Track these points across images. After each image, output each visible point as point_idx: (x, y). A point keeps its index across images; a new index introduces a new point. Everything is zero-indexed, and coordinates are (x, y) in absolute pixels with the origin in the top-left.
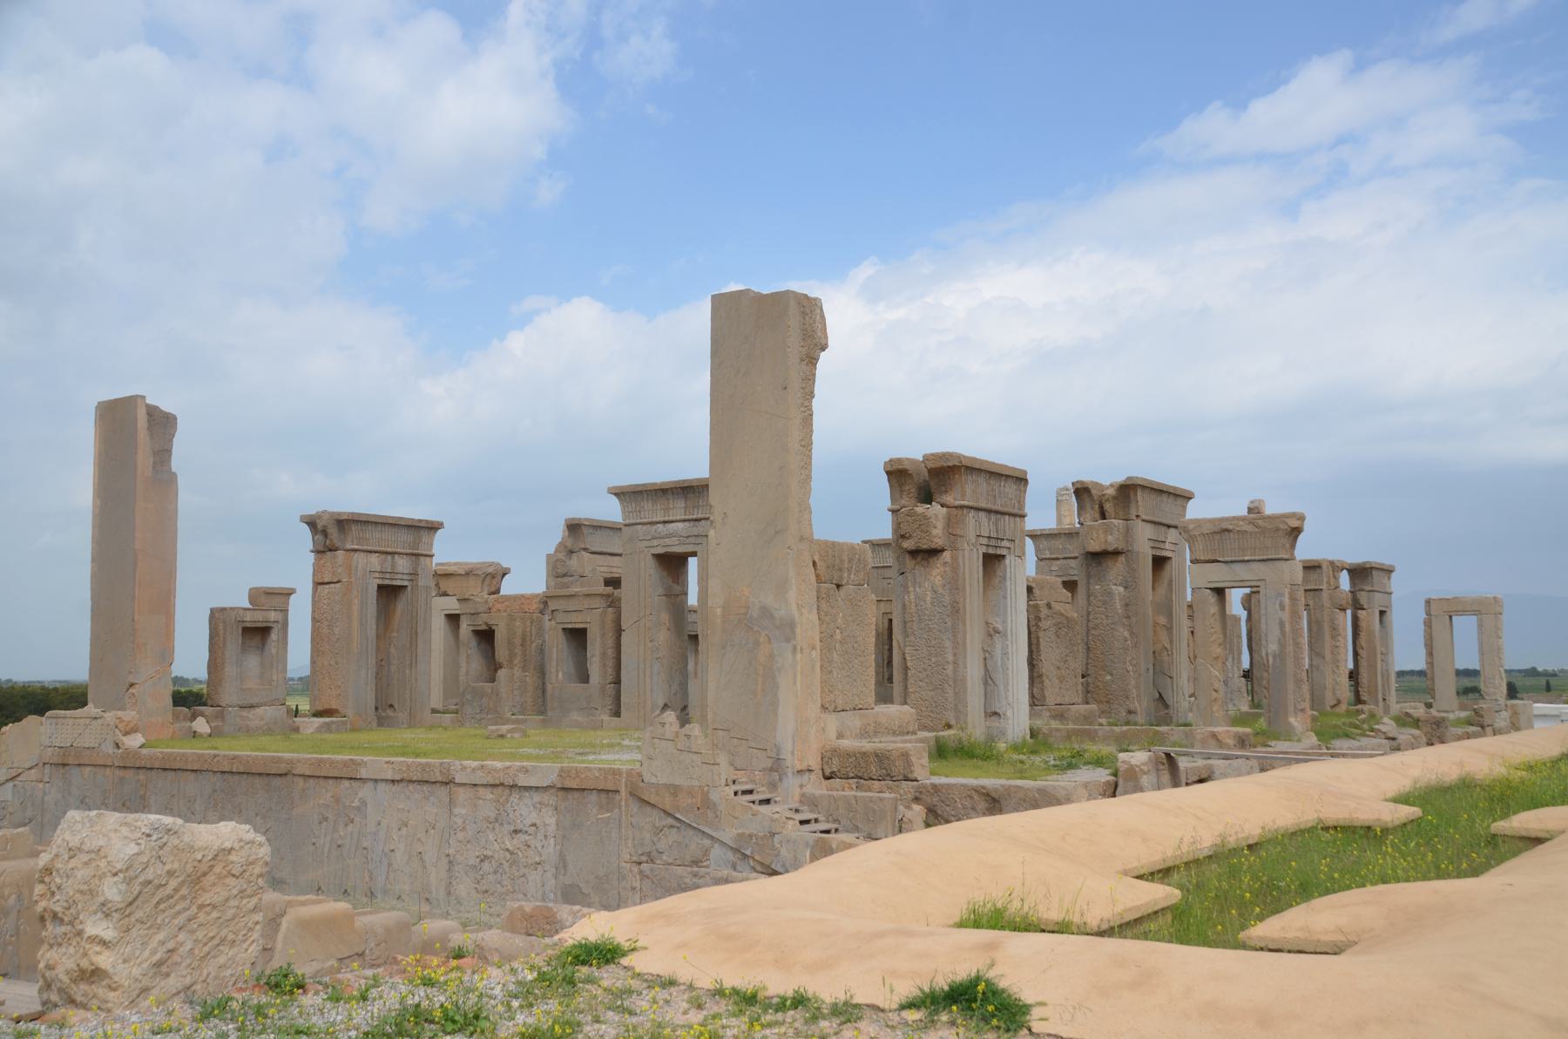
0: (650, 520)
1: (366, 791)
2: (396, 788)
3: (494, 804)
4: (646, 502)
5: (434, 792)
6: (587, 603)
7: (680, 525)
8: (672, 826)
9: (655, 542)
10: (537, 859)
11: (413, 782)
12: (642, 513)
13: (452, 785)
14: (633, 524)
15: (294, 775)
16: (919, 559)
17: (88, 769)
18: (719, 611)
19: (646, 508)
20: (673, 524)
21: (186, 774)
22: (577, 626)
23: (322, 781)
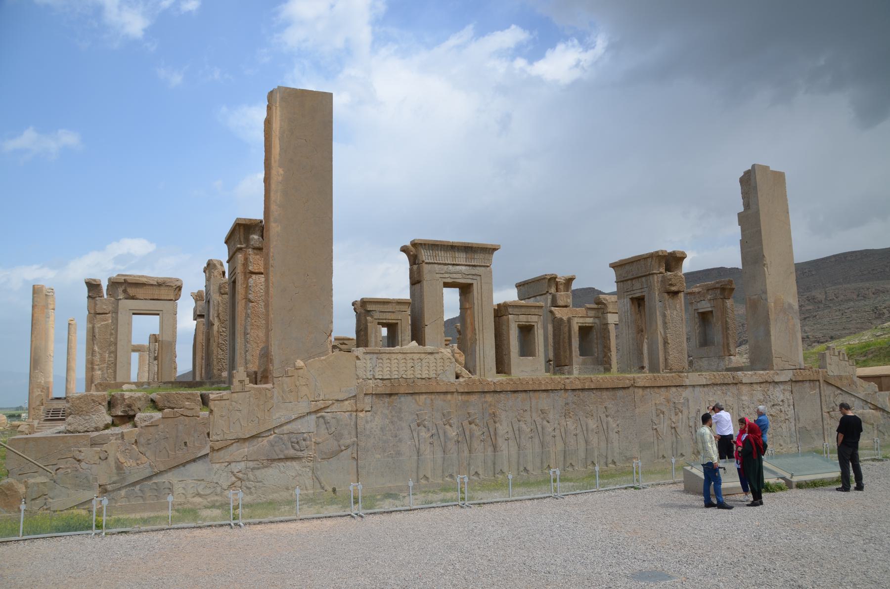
0: (444, 262)
1: (686, 393)
2: (706, 389)
3: (762, 392)
4: (439, 252)
5: (729, 389)
6: (398, 308)
7: (464, 268)
8: (841, 394)
9: (447, 275)
10: (787, 417)
11: (717, 384)
12: (437, 257)
13: (739, 384)
14: (432, 263)
15: (636, 387)
16: (671, 295)
17: (423, 397)
18: (773, 304)
19: (440, 254)
20: (457, 267)
21: (537, 394)
22: (390, 321)
23: (656, 390)
